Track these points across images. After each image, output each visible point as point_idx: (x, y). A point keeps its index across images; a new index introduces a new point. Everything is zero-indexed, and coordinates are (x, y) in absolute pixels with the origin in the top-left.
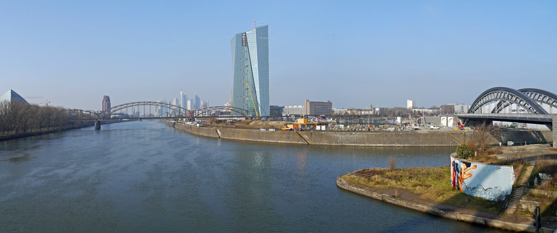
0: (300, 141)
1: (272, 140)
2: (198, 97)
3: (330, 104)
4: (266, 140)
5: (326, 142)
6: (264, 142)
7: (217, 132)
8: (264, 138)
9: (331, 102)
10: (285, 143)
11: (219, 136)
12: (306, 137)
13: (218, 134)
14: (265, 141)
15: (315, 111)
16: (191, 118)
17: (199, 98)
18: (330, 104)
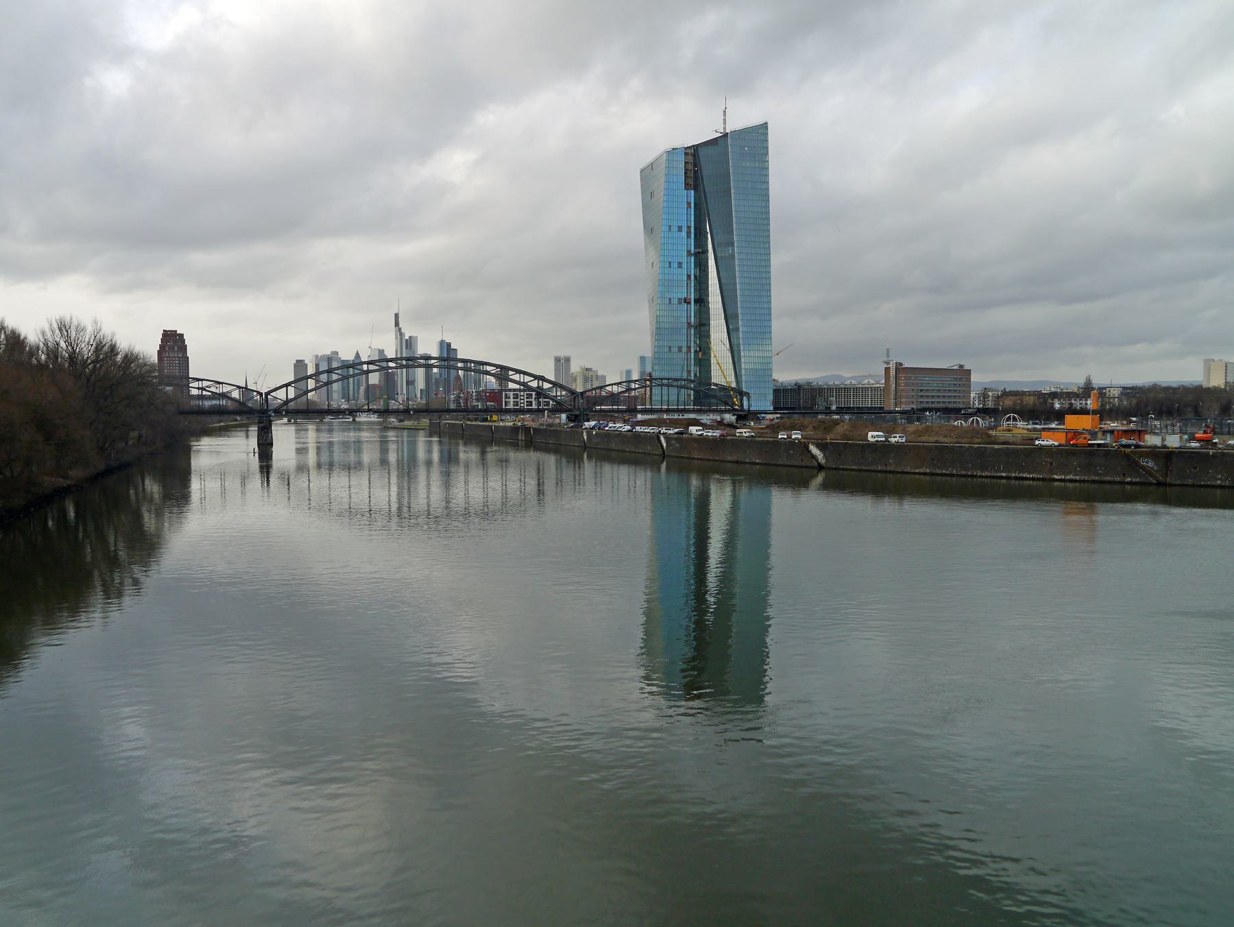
0: (1130, 476)
1: (1029, 473)
2: (452, 347)
3: (963, 374)
4: (1008, 472)
5: (1220, 479)
6: (1002, 478)
7: (810, 452)
8: (999, 467)
9: (966, 368)
10: (1075, 481)
11: (819, 464)
12: (1151, 464)
13: (814, 457)
14: (1004, 474)
15: (921, 396)
16: (578, 413)
17: (456, 350)
18: (963, 374)
